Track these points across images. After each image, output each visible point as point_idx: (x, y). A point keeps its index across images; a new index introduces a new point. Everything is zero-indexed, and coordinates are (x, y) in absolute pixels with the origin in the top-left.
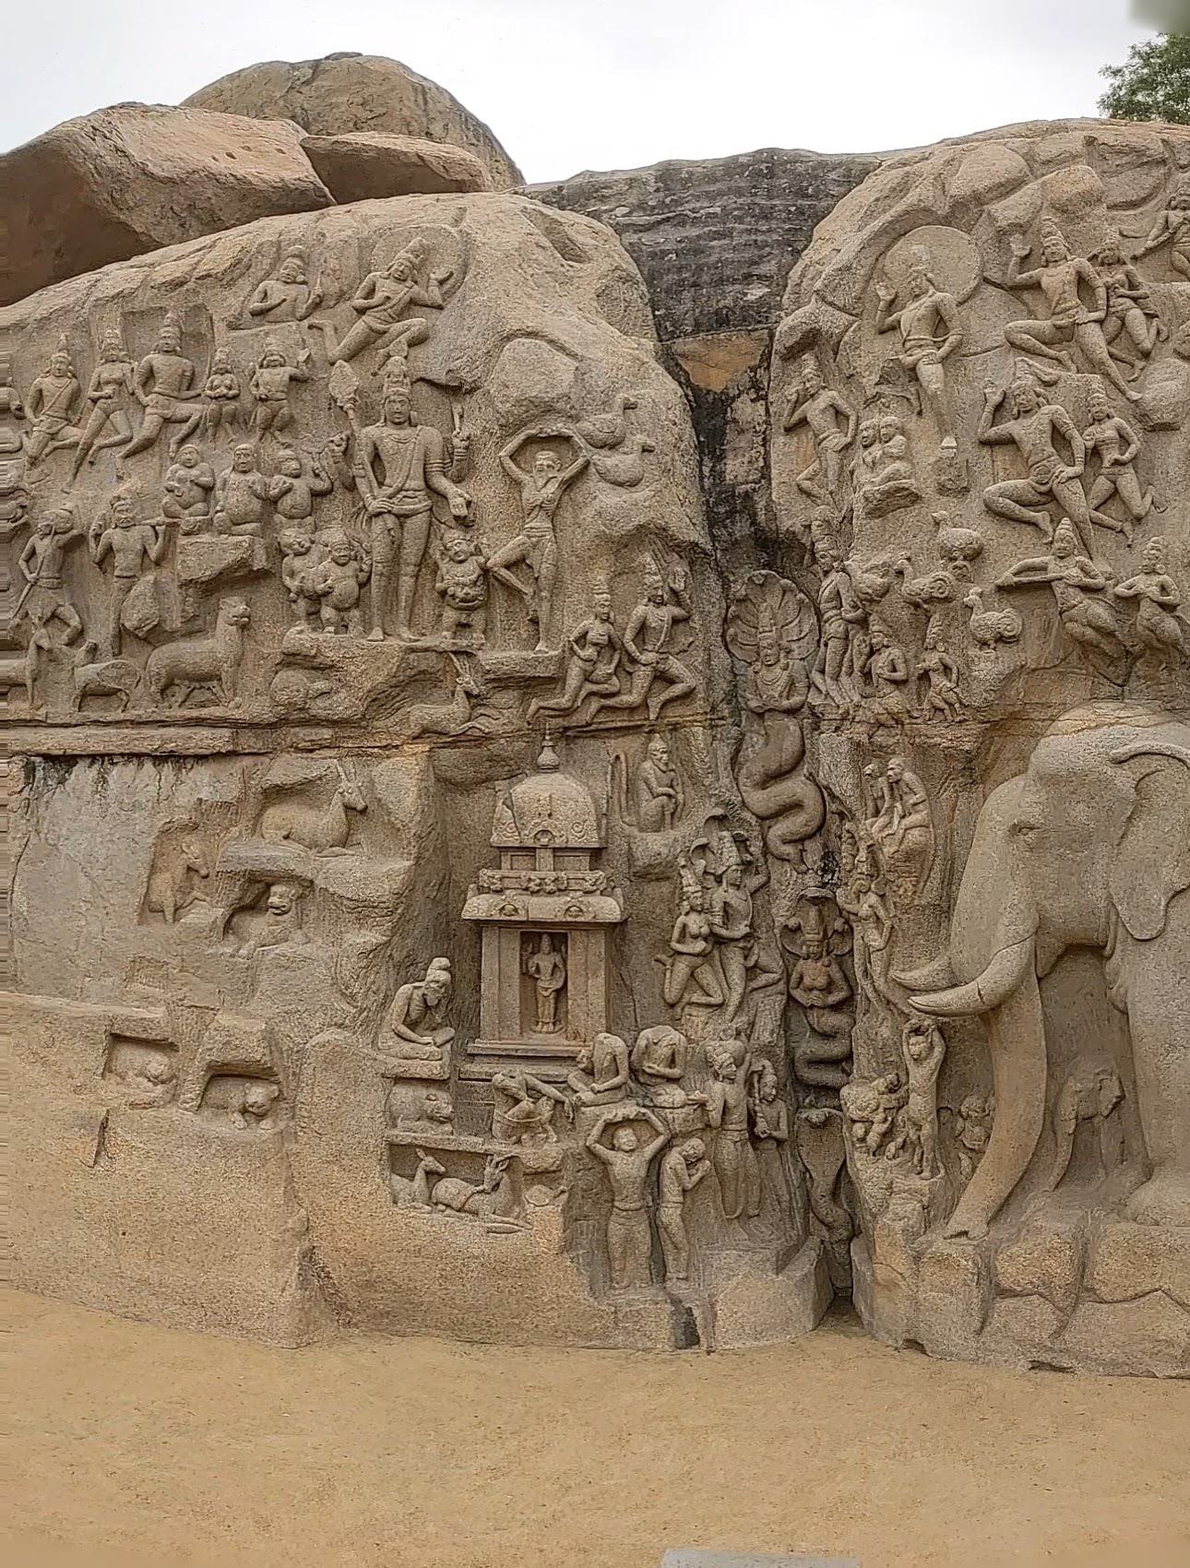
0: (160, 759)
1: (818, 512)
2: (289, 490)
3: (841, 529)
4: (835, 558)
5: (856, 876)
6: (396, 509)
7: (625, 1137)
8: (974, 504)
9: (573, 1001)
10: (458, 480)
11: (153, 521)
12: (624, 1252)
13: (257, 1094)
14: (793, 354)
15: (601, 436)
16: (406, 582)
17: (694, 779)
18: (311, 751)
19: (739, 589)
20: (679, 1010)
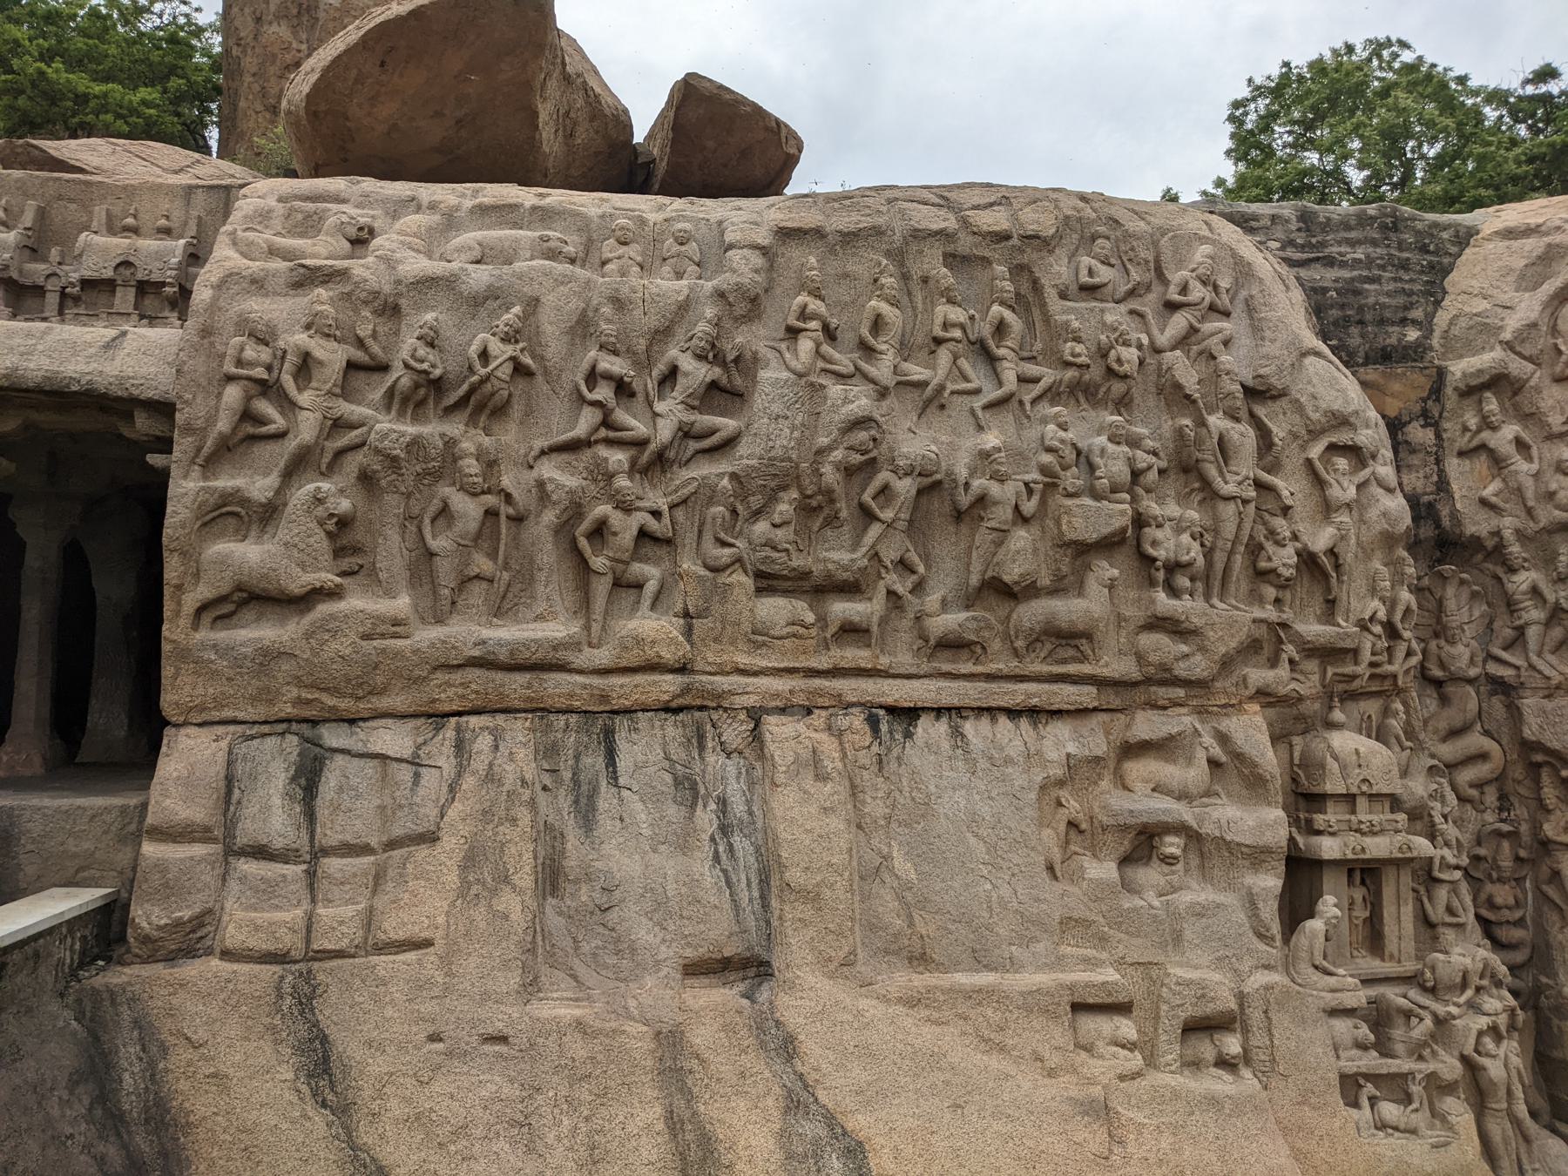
0: (1013, 713)
2: (1150, 468)
4: (1525, 560)
5: (1558, 812)
7: (1489, 1043)
9: (1390, 929)
11: (1028, 477)
14: (1472, 391)
16: (1238, 559)
18: (1165, 708)
20: (1441, 930)
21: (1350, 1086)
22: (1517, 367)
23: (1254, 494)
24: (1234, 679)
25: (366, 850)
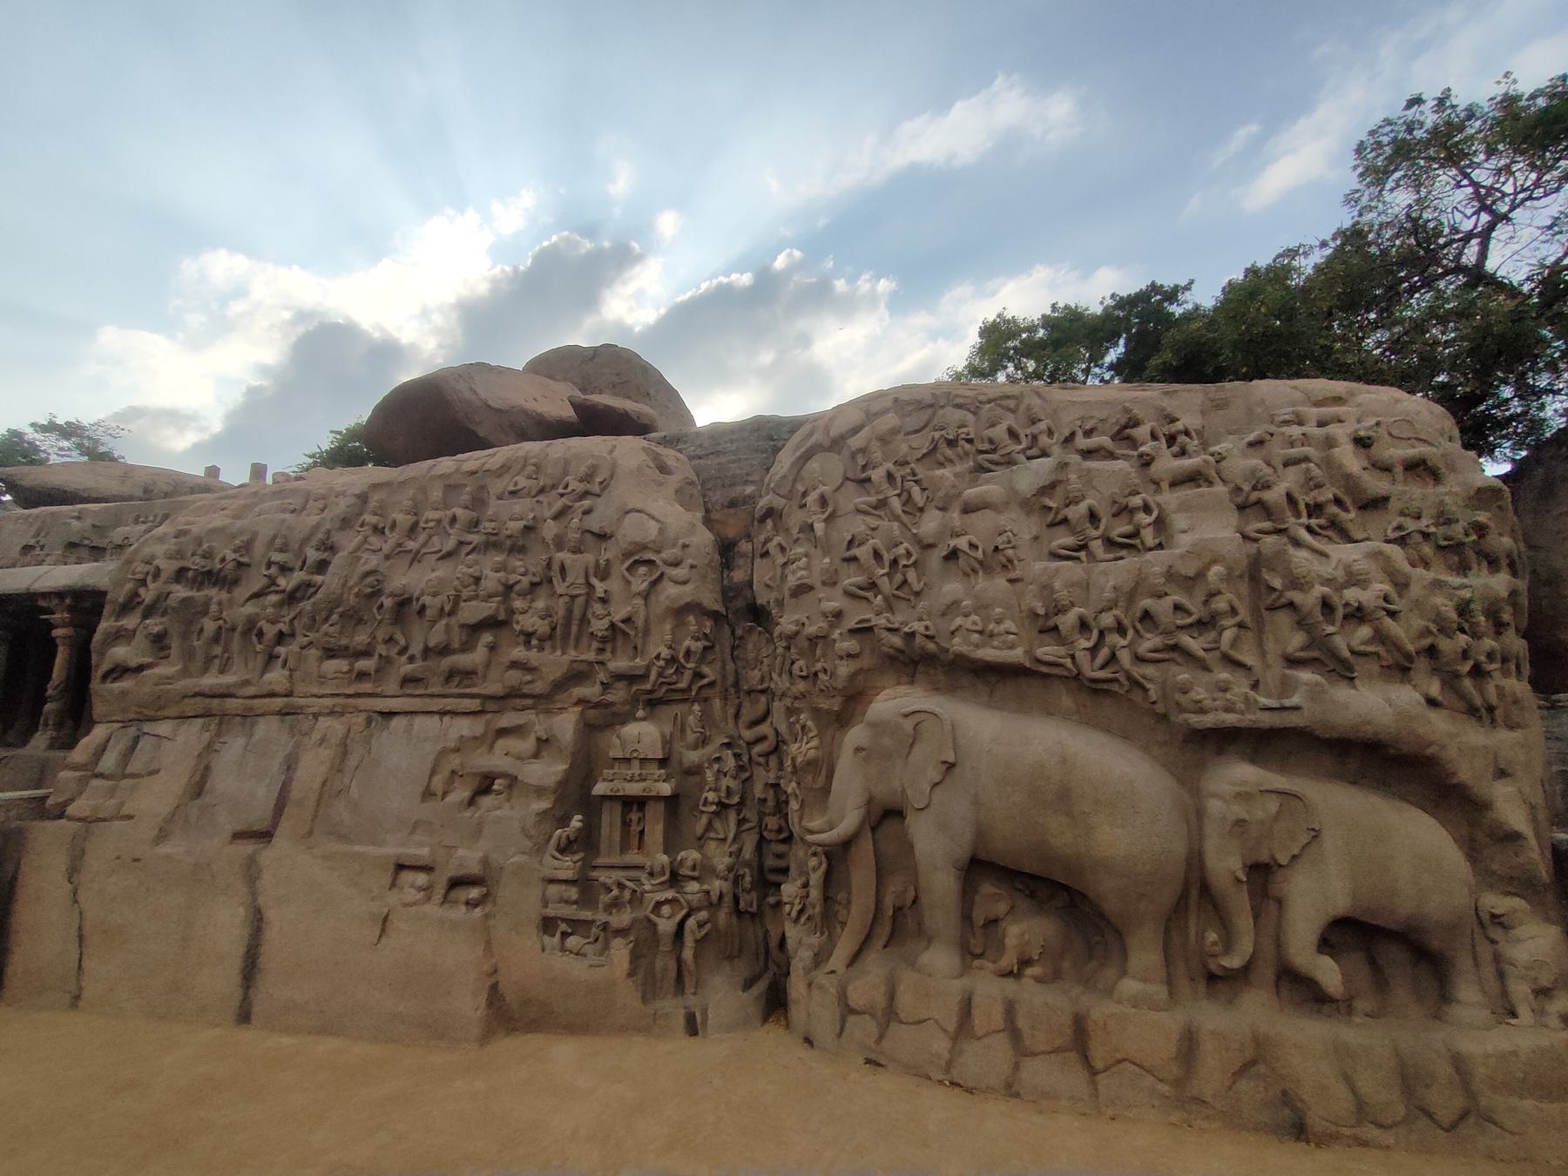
13: (474, 893)
16: (574, 629)
25: (132, 776)
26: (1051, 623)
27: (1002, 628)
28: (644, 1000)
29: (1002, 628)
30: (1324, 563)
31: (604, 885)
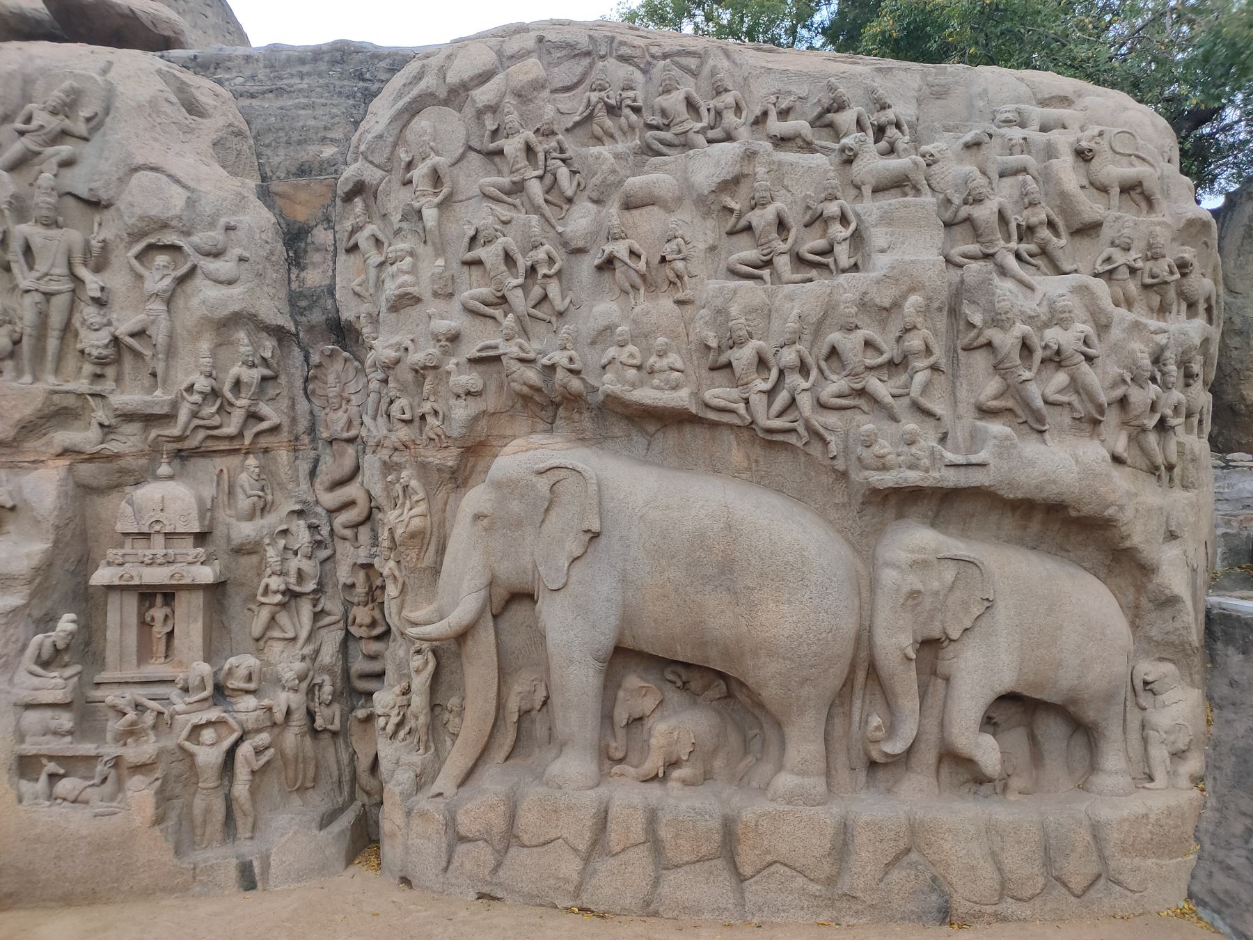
1: (365, 308)
3: (374, 320)
6: (43, 288)
8: (456, 305)
10: (98, 269)
12: (205, 822)
15: (207, 247)
16: (52, 344)
17: (281, 486)
19: (315, 358)
20: (262, 643)
21: (26, 766)
22: (371, 175)
23: (66, 286)
24: (43, 440)
26: (723, 359)
27: (664, 362)
28: (177, 852)
29: (664, 362)
30: (1032, 297)
31: (113, 707)
